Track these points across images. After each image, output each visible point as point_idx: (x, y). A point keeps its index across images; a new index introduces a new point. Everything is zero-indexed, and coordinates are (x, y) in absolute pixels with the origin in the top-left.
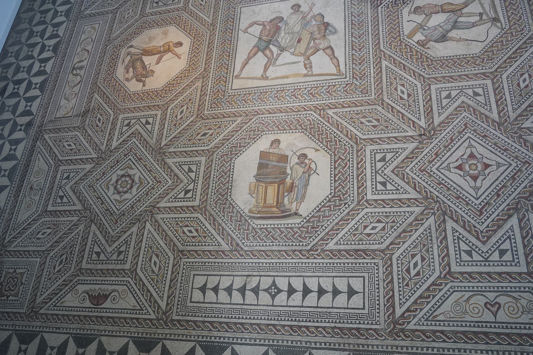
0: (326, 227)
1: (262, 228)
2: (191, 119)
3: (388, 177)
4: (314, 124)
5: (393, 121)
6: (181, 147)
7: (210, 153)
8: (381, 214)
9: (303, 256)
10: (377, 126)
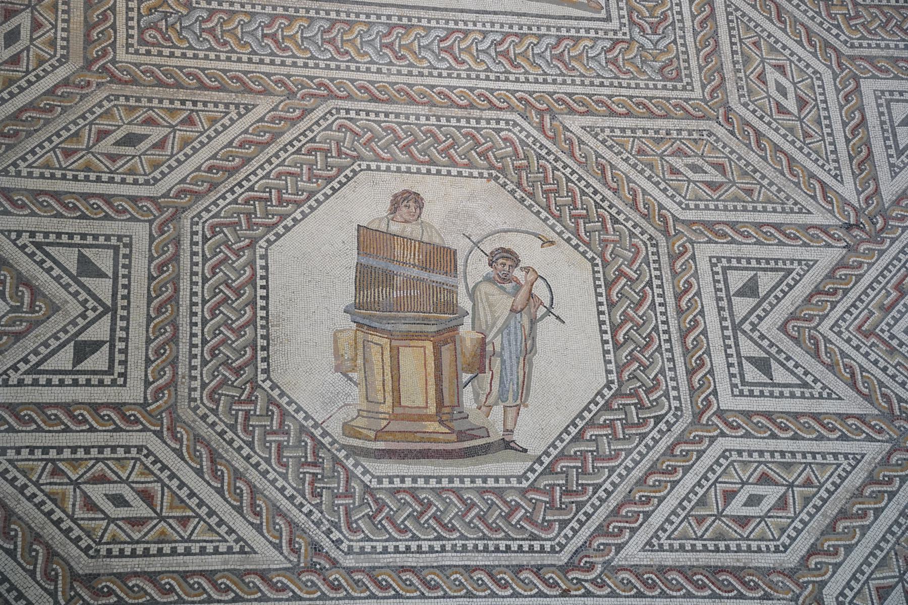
0: (609, 493)
1: (398, 491)
2: (62, 73)
3: (772, 345)
4: (526, 157)
5: (763, 177)
6: (30, 175)
7: (166, 213)
8: (767, 455)
9: (550, 586)
10: (721, 184)
